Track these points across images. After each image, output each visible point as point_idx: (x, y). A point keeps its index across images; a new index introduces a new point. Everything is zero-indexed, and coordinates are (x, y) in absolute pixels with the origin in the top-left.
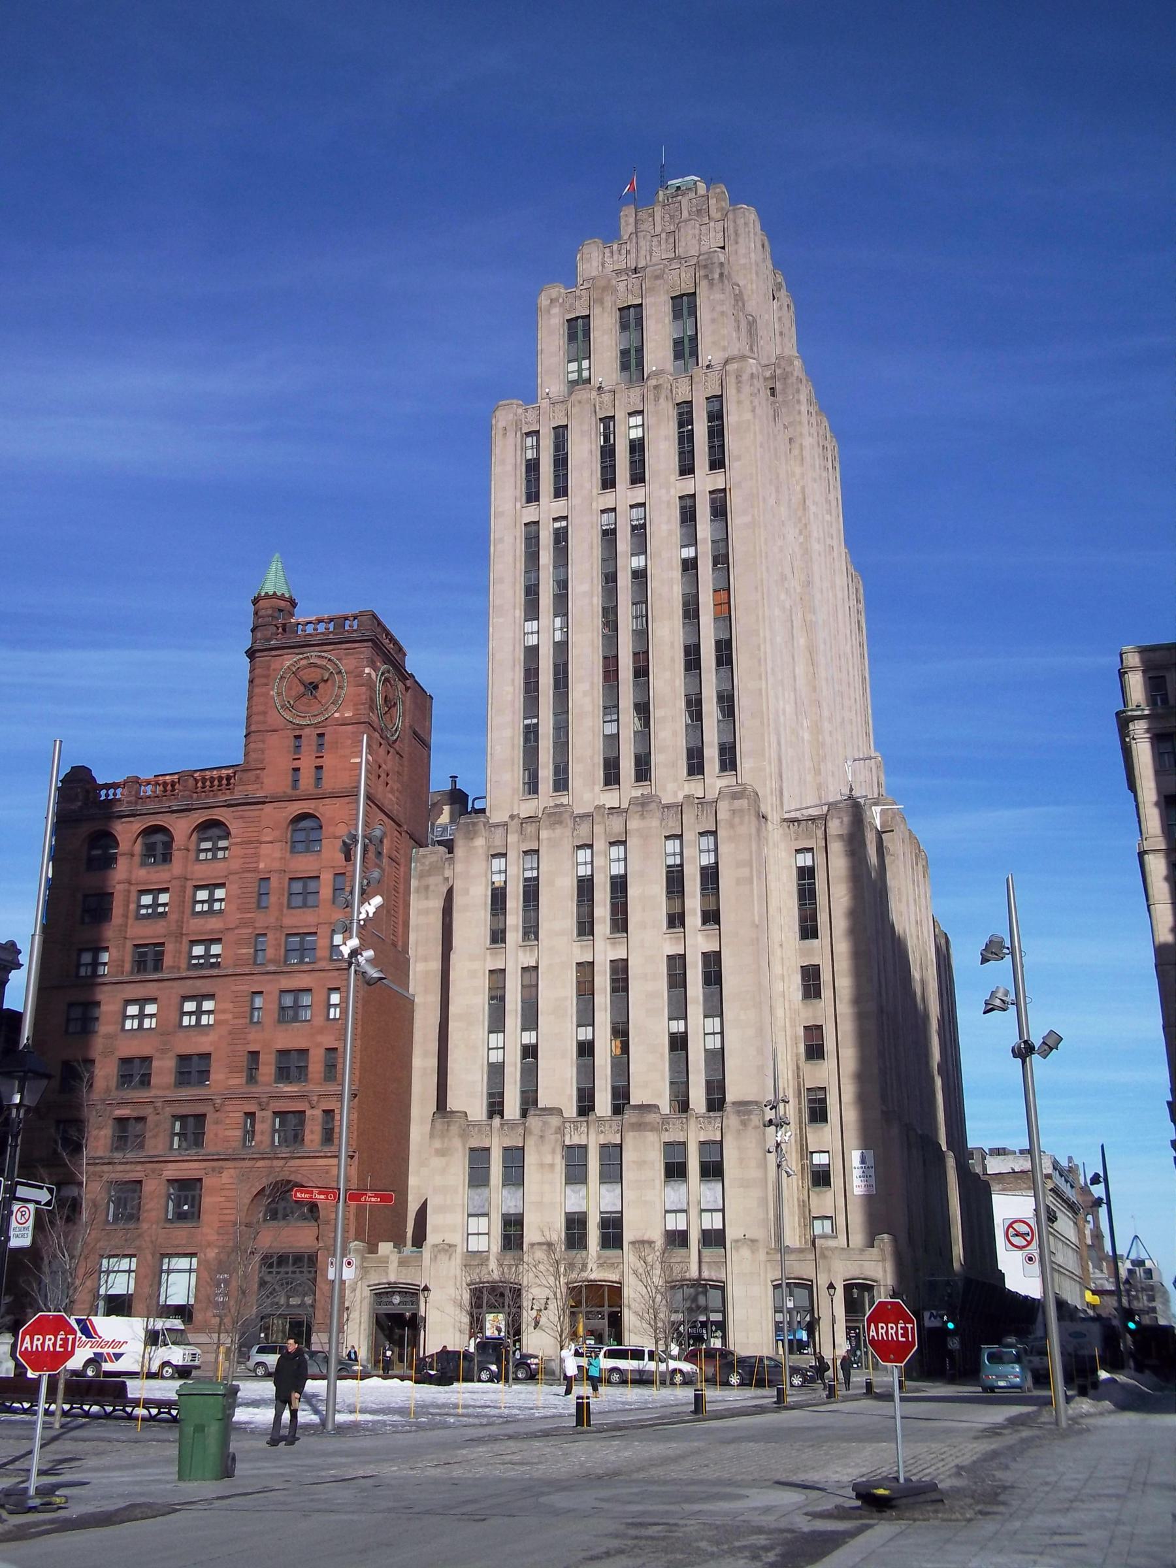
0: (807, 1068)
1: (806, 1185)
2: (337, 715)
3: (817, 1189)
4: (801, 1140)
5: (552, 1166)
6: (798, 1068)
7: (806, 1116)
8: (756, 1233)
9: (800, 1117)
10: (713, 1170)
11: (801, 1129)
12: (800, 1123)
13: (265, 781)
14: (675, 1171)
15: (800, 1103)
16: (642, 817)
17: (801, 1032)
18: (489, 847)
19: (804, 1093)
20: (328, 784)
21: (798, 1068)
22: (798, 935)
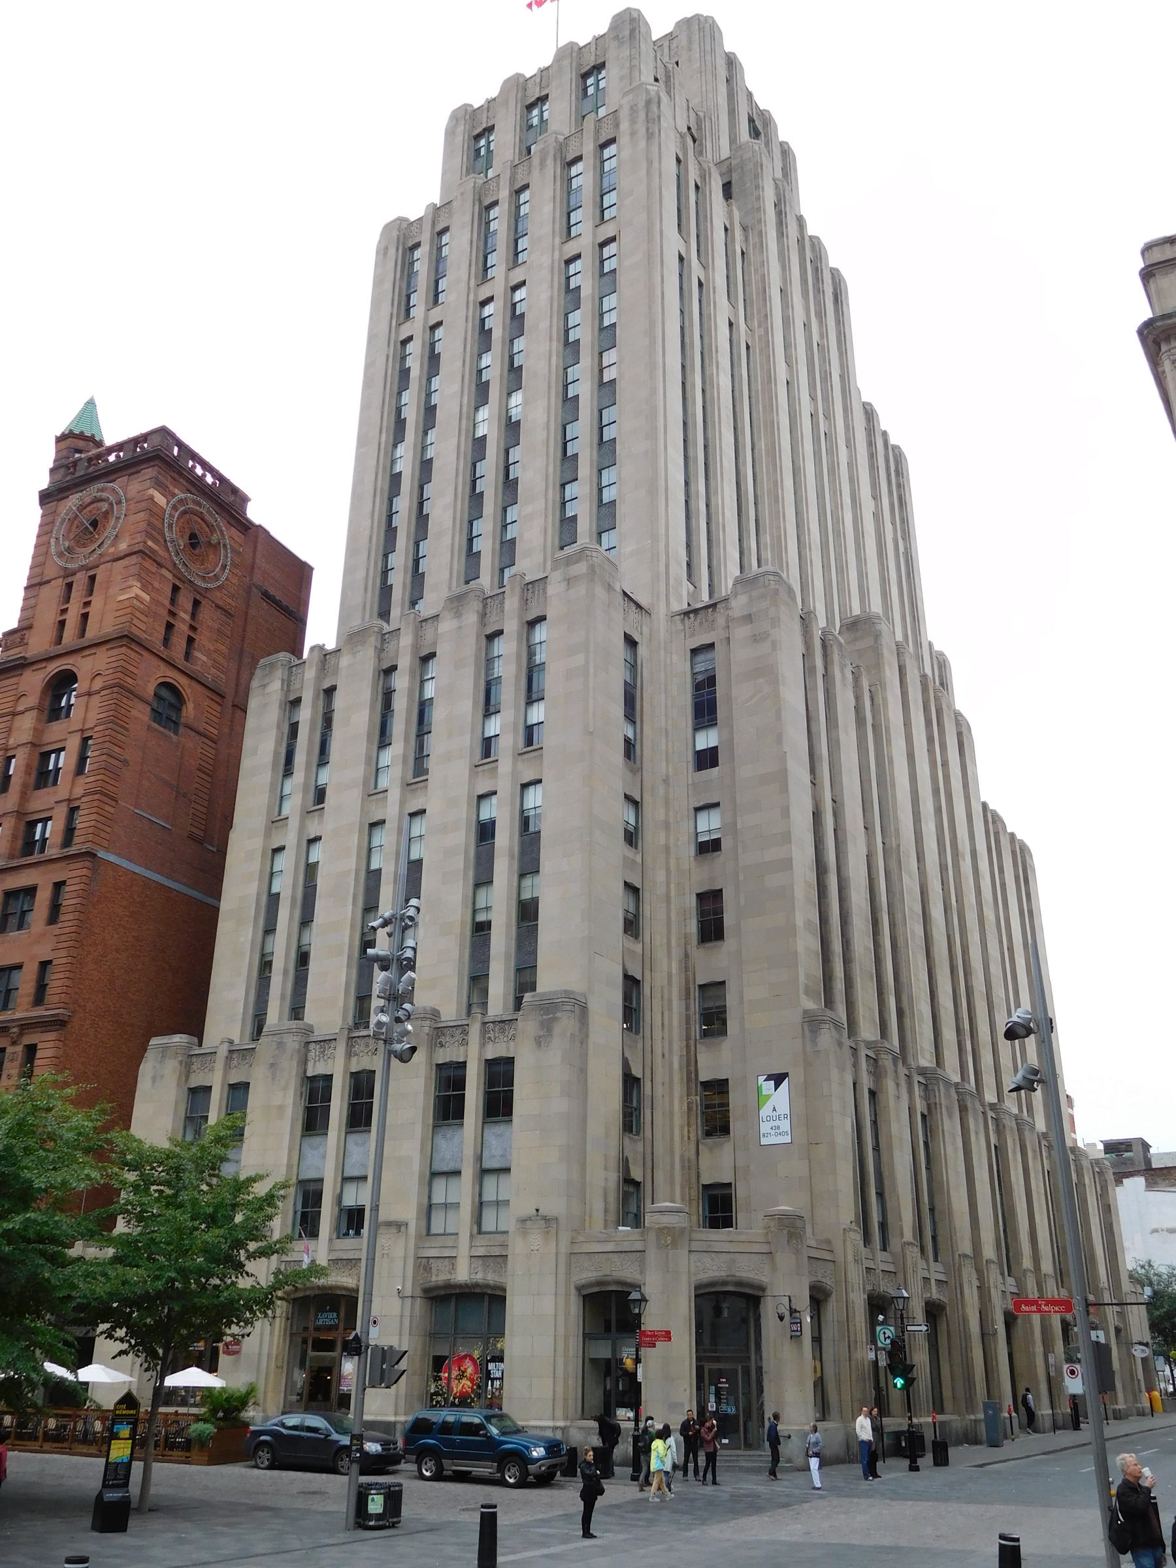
0: (699, 955)
1: (693, 1136)
2: (112, 550)
3: (709, 1141)
4: (688, 1065)
5: (281, 1108)
6: (687, 956)
7: (697, 1028)
8: (554, 1206)
9: (688, 1030)
10: (499, 1106)
11: (688, 1046)
12: (688, 1039)
13: (30, 641)
14: (448, 1108)
15: (687, 1008)
16: (458, 615)
17: (692, 902)
18: (289, 691)
19: (695, 993)
20: (92, 633)
21: (687, 956)
22: (691, 766)
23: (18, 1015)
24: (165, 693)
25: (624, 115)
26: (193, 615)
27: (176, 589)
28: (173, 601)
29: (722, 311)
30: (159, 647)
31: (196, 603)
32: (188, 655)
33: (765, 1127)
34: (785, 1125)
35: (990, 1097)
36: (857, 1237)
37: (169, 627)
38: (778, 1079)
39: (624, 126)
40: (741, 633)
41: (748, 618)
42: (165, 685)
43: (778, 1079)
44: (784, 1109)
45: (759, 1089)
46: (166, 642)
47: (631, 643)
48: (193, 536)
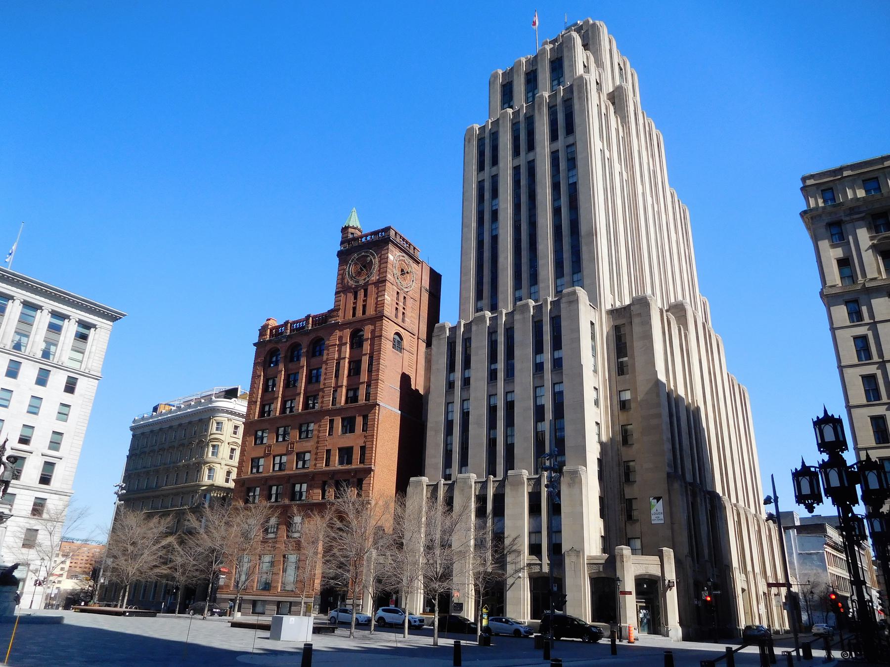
23: (353, 467)
24: (397, 337)
25: (575, 88)
26: (404, 304)
27: (398, 293)
28: (398, 299)
29: (617, 167)
30: (394, 319)
31: (405, 298)
32: (403, 321)
33: (653, 517)
34: (662, 516)
35: (734, 501)
36: (689, 559)
37: (397, 309)
38: (658, 499)
39: (575, 94)
40: (636, 321)
41: (639, 315)
42: (397, 334)
43: (658, 499)
44: (661, 509)
45: (650, 503)
46: (396, 316)
47: (592, 324)
48: (402, 270)
